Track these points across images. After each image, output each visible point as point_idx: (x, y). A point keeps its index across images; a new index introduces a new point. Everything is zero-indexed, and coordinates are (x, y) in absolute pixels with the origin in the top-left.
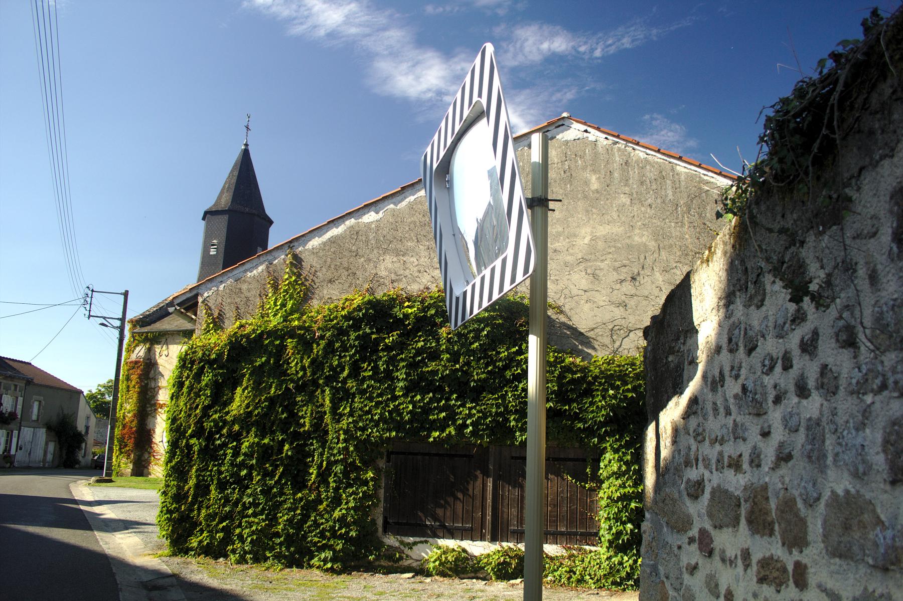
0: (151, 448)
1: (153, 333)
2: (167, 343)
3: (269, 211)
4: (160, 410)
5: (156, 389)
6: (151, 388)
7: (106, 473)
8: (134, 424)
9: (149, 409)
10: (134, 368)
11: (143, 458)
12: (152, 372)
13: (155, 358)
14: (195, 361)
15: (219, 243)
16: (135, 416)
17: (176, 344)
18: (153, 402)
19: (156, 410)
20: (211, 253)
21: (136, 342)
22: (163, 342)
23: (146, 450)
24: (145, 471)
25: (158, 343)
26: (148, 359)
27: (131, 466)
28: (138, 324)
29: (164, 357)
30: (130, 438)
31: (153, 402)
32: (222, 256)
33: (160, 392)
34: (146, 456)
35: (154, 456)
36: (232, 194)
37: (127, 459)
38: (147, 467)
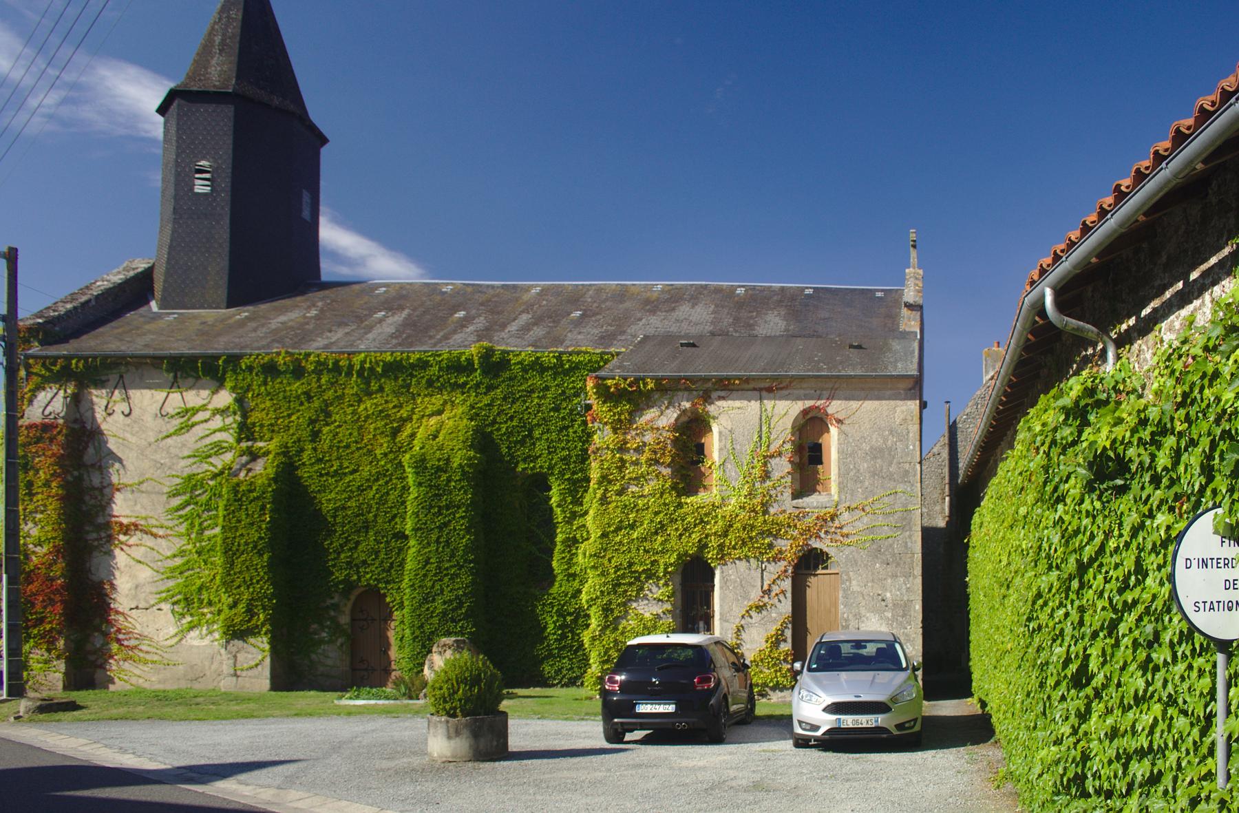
0: (109, 623)
1: (86, 358)
2: (123, 384)
3: (318, 112)
4: (122, 537)
5: (107, 491)
6: (94, 488)
7: (9, 686)
8: (57, 570)
9: (94, 535)
10: (39, 440)
11: (89, 647)
12: (91, 450)
13: (94, 418)
14: (1164, 667)
15: (215, 171)
16: (57, 551)
17: (149, 387)
18: (101, 520)
19: (110, 538)
20: (198, 189)
21: (36, 379)
22: (113, 382)
23: (98, 629)
24: (99, 674)
25: (100, 384)
26: (75, 421)
27: (61, 665)
28: (36, 337)
29: (118, 417)
30: (52, 602)
31: (101, 520)
32: (225, 196)
33: (119, 497)
34: (98, 641)
35: (118, 641)
36: (234, 58)
37: (49, 651)
38: (102, 667)
